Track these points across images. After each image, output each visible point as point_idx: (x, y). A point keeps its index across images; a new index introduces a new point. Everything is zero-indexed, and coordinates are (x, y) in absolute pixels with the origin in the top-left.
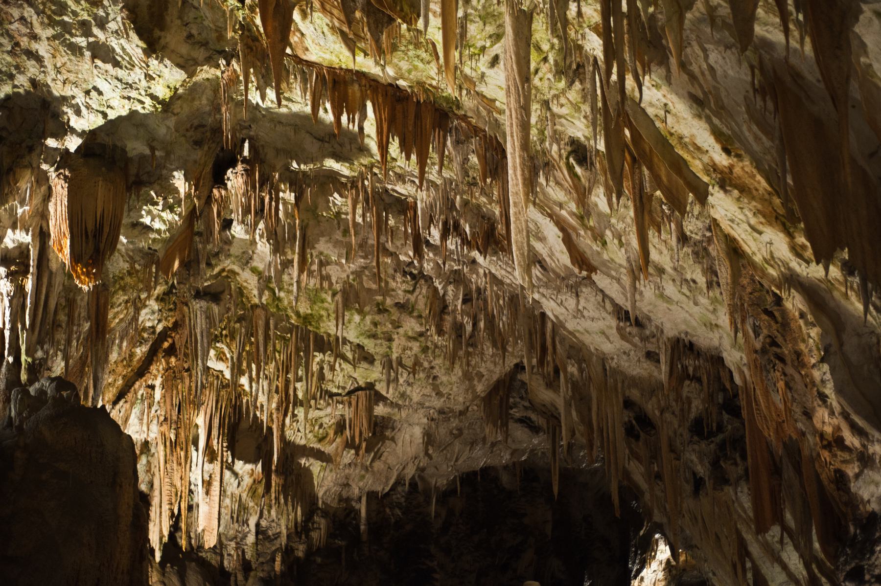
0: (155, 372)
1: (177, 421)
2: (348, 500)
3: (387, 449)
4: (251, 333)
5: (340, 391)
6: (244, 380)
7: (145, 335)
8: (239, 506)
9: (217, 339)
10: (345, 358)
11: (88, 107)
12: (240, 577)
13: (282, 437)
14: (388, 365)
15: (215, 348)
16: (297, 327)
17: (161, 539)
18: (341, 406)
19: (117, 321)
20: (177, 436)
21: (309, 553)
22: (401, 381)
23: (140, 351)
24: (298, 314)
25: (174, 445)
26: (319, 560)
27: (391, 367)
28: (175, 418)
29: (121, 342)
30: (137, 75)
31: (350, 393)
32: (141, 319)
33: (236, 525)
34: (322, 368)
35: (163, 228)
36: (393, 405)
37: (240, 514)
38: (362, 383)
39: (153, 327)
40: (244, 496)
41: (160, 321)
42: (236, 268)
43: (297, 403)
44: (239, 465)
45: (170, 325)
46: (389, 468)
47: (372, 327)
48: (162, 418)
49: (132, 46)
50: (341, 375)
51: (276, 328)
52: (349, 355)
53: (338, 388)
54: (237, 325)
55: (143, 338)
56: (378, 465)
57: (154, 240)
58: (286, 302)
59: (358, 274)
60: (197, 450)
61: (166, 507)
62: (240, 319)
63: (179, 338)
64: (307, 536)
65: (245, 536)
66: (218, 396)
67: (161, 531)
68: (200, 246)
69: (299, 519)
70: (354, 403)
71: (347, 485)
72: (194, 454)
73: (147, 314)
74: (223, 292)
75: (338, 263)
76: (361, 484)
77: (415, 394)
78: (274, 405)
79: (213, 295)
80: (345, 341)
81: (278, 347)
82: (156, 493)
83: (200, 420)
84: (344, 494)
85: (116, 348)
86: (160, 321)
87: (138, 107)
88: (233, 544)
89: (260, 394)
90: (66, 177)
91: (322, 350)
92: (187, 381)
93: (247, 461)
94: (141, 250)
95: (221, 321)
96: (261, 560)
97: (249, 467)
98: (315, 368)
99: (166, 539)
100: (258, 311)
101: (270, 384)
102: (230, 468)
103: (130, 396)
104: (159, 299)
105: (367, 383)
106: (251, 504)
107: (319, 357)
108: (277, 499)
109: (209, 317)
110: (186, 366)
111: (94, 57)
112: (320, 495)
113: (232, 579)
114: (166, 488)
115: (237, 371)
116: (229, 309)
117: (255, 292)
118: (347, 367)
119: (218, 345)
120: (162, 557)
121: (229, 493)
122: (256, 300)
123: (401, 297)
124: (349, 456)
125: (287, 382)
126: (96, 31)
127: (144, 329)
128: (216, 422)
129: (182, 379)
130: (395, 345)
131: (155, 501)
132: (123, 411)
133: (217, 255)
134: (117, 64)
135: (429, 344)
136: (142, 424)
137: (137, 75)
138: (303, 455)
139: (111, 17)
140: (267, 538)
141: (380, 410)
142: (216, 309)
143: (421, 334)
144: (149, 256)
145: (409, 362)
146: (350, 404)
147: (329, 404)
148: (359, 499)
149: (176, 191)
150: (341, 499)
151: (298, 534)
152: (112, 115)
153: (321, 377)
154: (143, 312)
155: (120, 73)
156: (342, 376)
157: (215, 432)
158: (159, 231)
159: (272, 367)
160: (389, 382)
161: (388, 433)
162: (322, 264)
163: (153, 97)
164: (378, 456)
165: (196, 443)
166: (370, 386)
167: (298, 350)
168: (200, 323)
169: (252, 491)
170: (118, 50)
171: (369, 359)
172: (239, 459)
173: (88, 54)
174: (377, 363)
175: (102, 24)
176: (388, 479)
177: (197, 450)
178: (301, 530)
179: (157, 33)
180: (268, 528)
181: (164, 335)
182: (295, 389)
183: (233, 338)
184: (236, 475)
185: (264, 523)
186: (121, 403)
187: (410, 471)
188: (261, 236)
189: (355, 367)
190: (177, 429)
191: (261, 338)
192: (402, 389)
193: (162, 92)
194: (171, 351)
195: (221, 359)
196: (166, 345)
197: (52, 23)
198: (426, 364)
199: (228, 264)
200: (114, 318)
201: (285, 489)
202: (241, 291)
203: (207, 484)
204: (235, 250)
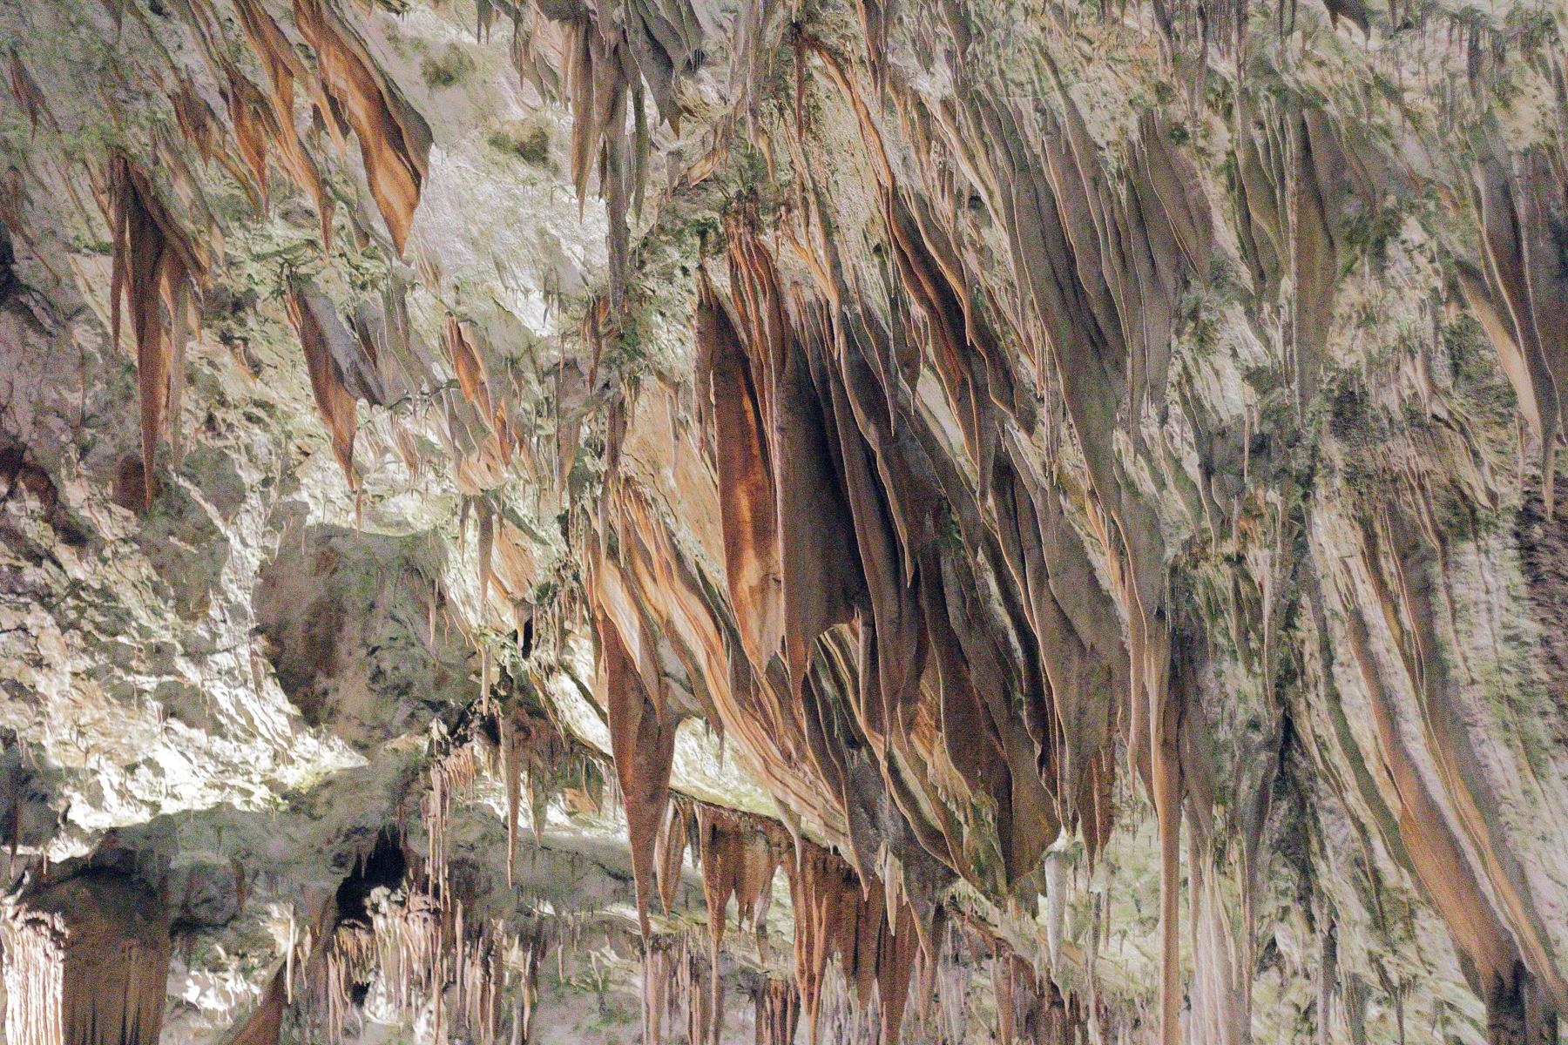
11: (123, 793)
30: (258, 756)
35: (222, 1007)
49: (272, 708)
87: (237, 801)
90: (56, 935)
111: (170, 713)
126: (181, 664)
134: (217, 730)
137: (258, 756)
139: (225, 641)
149: (270, 942)
152: (169, 807)
155: (218, 744)
158: (210, 1015)
163: (272, 785)
170: (225, 703)
173: (155, 706)
175: (197, 655)
179: (322, 682)
193: (295, 777)
197: (90, 645)
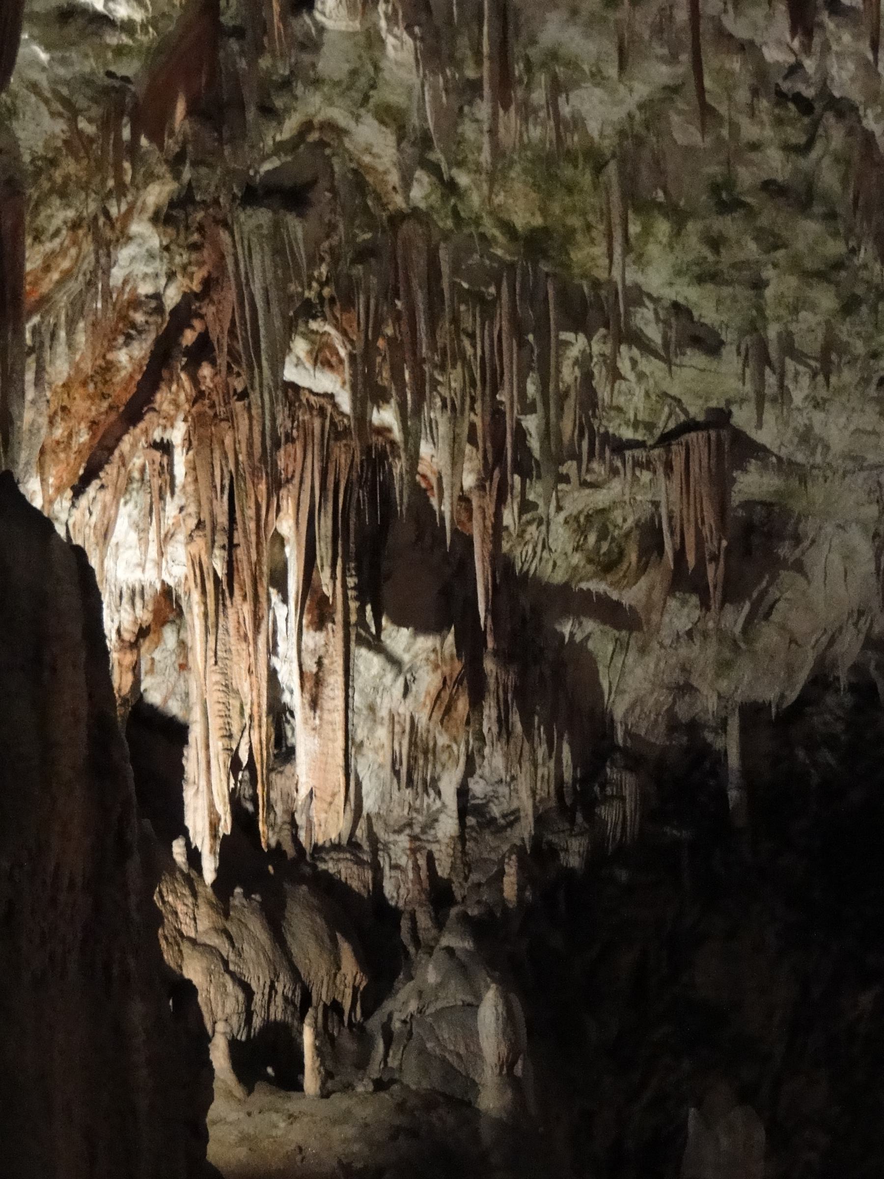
0: (167, 407)
1: (227, 530)
2: (694, 727)
3: (787, 590)
4: (391, 292)
5: (639, 437)
6: (385, 416)
7: (139, 317)
8: (413, 744)
9: (309, 310)
10: (636, 339)
12: (424, 920)
13: (502, 565)
14: (759, 357)
15: (309, 335)
16: (512, 266)
17: (214, 827)
18: (645, 476)
19: (55, 276)
20: (231, 565)
21: (597, 857)
22: (798, 397)
23: (129, 358)
24: (508, 228)
25: (222, 590)
26: (623, 875)
27: (765, 360)
28: (223, 520)
29: (71, 332)
31: (666, 439)
32: (117, 274)
33: (408, 793)
34: (588, 376)
36: (786, 467)
37: (414, 765)
38: (696, 411)
39: (157, 296)
40: (422, 718)
41: (171, 276)
42: (338, 115)
43: (525, 467)
44: (398, 638)
45: (196, 287)
46: (792, 641)
47: (706, 252)
48: (192, 523)
50: (639, 392)
51: (456, 270)
52: (654, 333)
53: (636, 425)
54: (358, 270)
55: (133, 325)
56: (769, 636)
57: (120, 51)
58: (475, 199)
59: (653, 111)
60: (285, 601)
61: (217, 745)
62: (364, 254)
63: (215, 317)
64: (590, 817)
65: (433, 821)
66: (326, 459)
67: (212, 805)
68: (243, 64)
69: (568, 776)
70: (678, 464)
71: (684, 689)
72: (281, 611)
73: (133, 259)
74: (311, 184)
75: (598, 77)
76: (724, 685)
77: (836, 429)
78: (469, 480)
79: (290, 196)
80: (637, 296)
81: (467, 323)
82: (196, 715)
83: (286, 525)
84: (683, 712)
85: (61, 348)
86: (171, 276)
88: (403, 840)
89: (440, 461)
91: (579, 322)
92: (243, 423)
93: (421, 628)
94: (87, 81)
95: (314, 260)
96: (475, 877)
97: (426, 643)
98: (569, 374)
99: (226, 827)
100: (407, 228)
101: (454, 421)
102: (376, 645)
103: (110, 472)
104: (162, 219)
105: (710, 411)
106: (443, 740)
107: (577, 344)
108: (503, 722)
109: (280, 249)
110: (239, 384)
112: (619, 713)
113: (405, 924)
114: (214, 696)
115: (368, 392)
116: (332, 227)
117: (394, 178)
118: (651, 366)
119: (314, 325)
120: (218, 871)
121: (383, 713)
122: (399, 200)
123: (775, 163)
124: (680, 615)
125: (497, 414)
127: (136, 303)
128: (325, 526)
129: (230, 418)
130: (769, 292)
131: (195, 734)
132: (97, 509)
133: (286, 85)
135: (860, 290)
136: (144, 541)
138: (566, 613)
140: (488, 823)
141: (752, 483)
142: (296, 227)
143: (838, 265)
144: (113, 97)
145: (811, 344)
146: (669, 467)
147: (614, 472)
148: (723, 724)
150: (674, 726)
151: (565, 811)
153: (589, 400)
154: (124, 254)
156: (638, 392)
157: (323, 550)
158: (128, 27)
159: (455, 378)
160: (760, 399)
161: (784, 550)
162: (557, 88)
164: (761, 612)
165: (279, 581)
166: (719, 418)
167: (518, 329)
168: (260, 273)
169: (442, 704)
171: (707, 342)
172: (399, 621)
174: (729, 353)
176: (791, 670)
177: (285, 601)
178: (573, 803)
180: (489, 799)
181: (183, 315)
182: (521, 434)
183: (349, 303)
184: (394, 661)
185: (478, 787)
186: (92, 490)
187: (849, 647)
188: (391, 19)
189: (668, 362)
190: (231, 547)
191: (420, 298)
192: (800, 421)
194: (203, 350)
195: (328, 364)
196: (189, 337)
198: (860, 348)
199: (313, 105)
200: (47, 268)
201: (523, 696)
202: (359, 180)
203: (313, 683)
204: (332, 63)
